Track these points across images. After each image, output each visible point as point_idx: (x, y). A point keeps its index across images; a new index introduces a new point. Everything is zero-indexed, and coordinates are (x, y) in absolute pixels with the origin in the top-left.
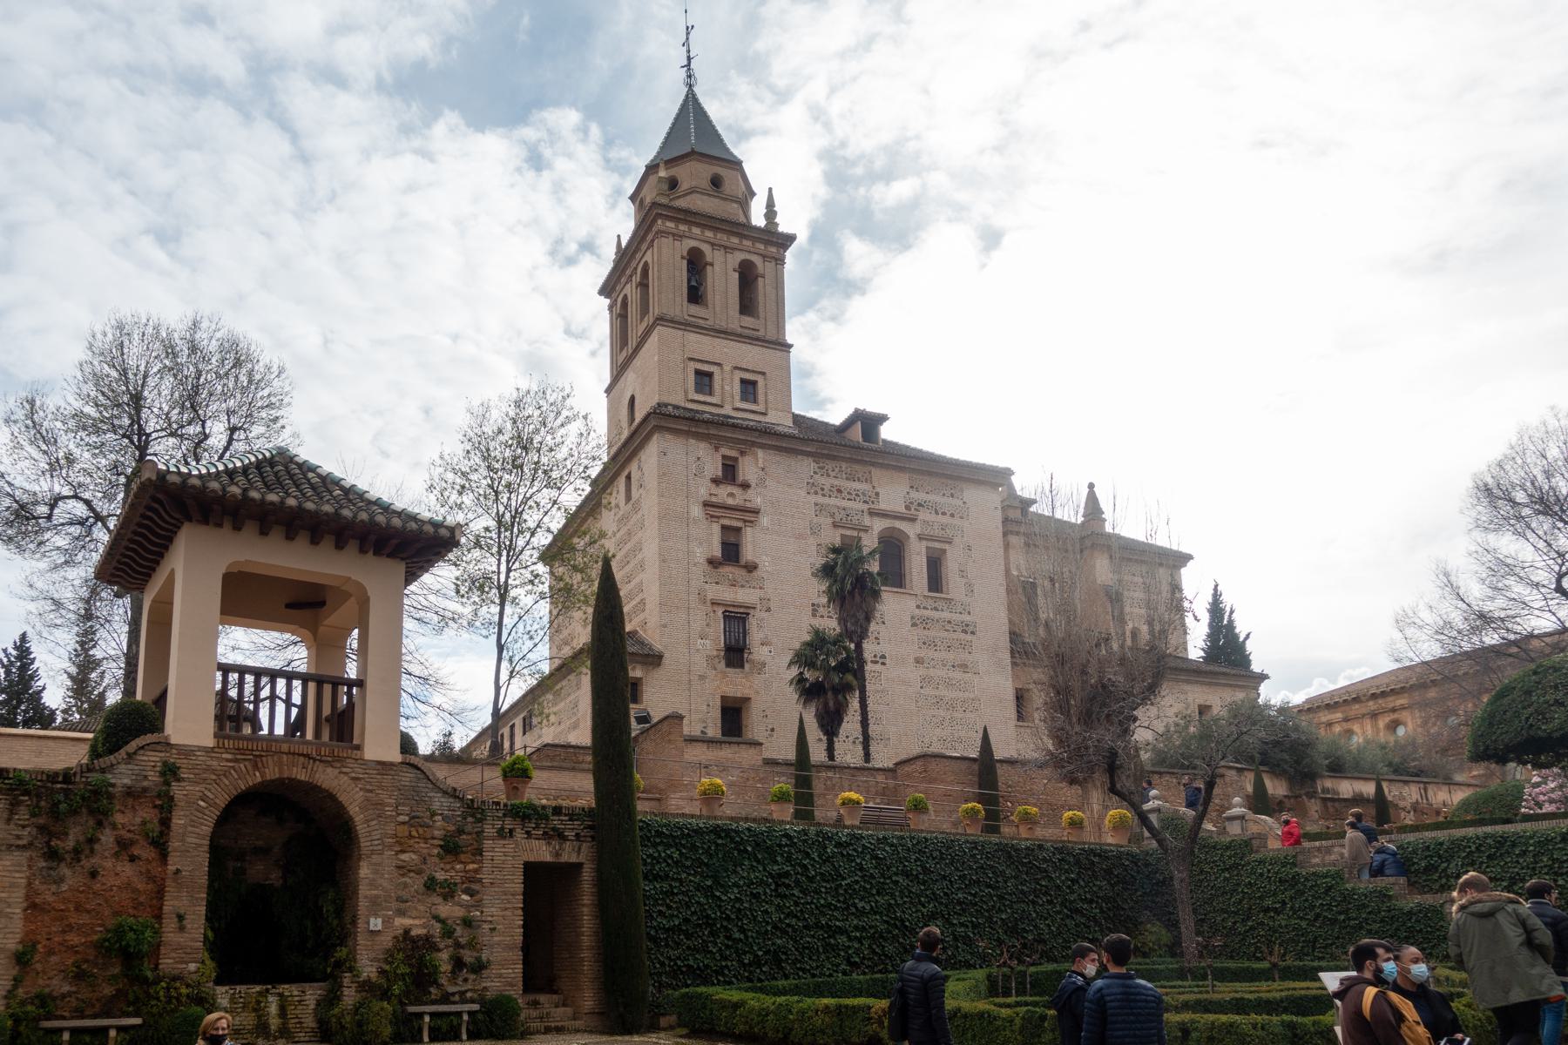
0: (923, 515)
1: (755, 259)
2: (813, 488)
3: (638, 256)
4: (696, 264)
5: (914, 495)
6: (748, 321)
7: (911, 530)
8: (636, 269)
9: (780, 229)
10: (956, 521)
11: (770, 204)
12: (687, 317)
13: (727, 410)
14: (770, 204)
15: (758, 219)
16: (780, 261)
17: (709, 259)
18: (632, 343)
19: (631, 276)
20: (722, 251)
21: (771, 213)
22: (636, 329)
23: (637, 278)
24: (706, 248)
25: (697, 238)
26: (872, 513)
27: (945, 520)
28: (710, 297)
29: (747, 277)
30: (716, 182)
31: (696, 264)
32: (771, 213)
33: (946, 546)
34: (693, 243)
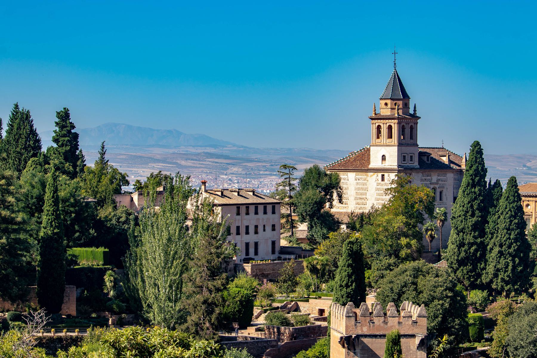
0: (440, 182)
2: (422, 180)
5: (439, 178)
6: (412, 141)
7: (437, 186)
9: (417, 115)
10: (445, 182)
11: (415, 107)
13: (408, 164)
14: (415, 107)
15: (411, 111)
16: (417, 123)
21: (415, 110)
26: (431, 184)
27: (443, 182)
29: (412, 128)
32: (415, 110)
33: (443, 189)
34: (402, 124)
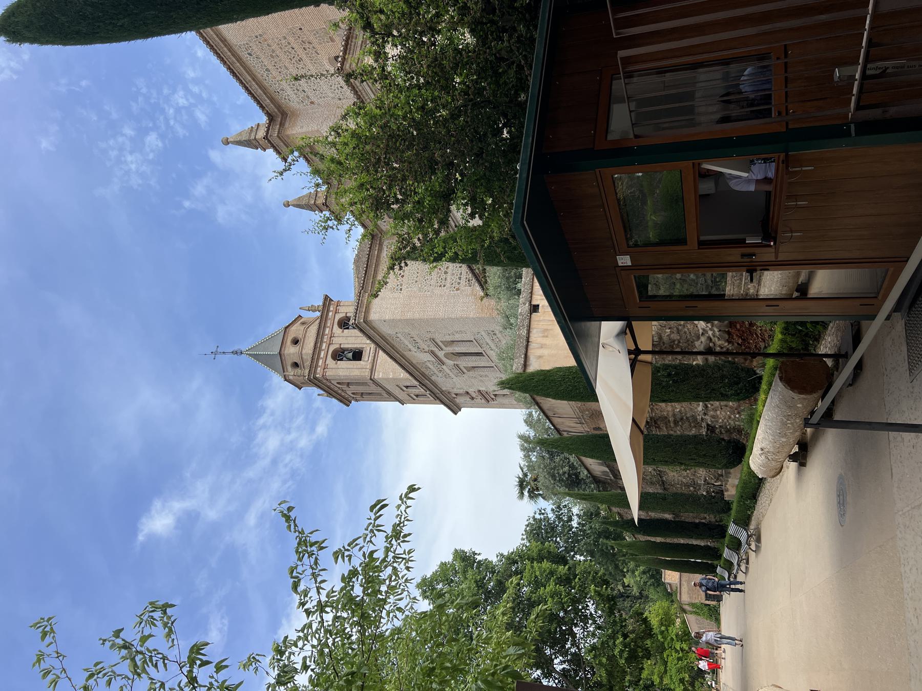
1: (336, 320)
3: (332, 387)
4: (339, 355)
8: (339, 388)
12: (370, 361)
17: (338, 346)
18: (379, 390)
19: (343, 390)
20: (332, 339)
22: (373, 388)
23: (344, 387)
24: (332, 349)
25: (326, 350)
28: (358, 346)
30: (296, 342)
31: (339, 355)
